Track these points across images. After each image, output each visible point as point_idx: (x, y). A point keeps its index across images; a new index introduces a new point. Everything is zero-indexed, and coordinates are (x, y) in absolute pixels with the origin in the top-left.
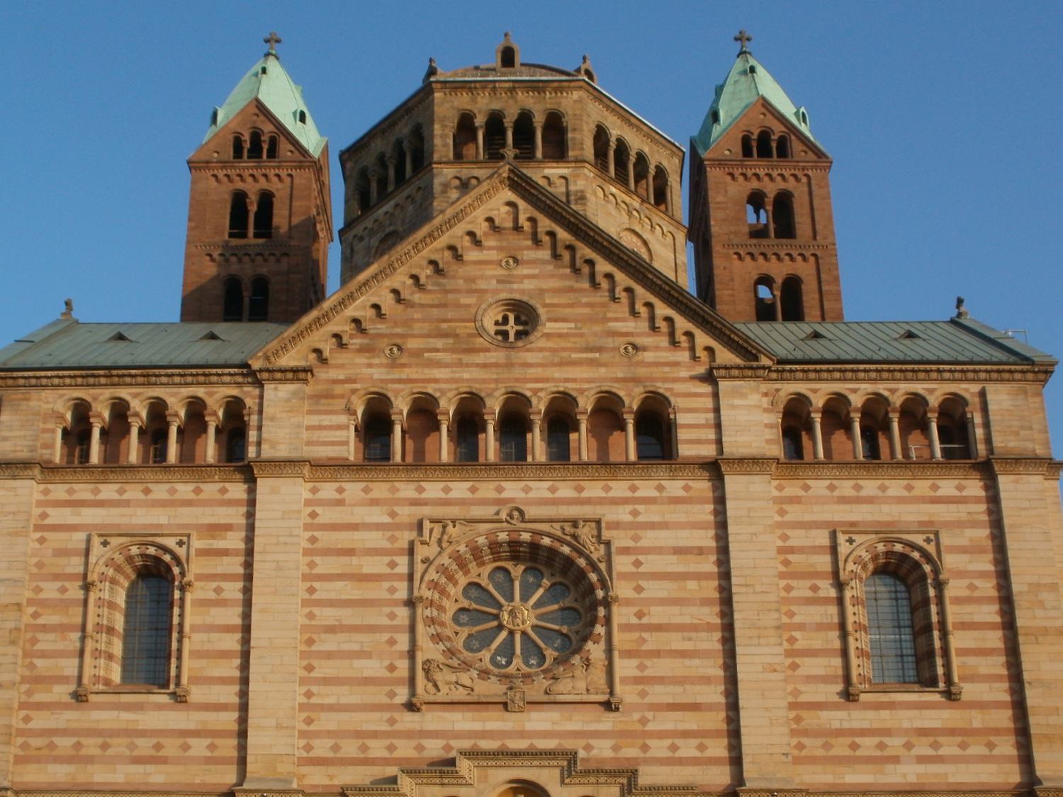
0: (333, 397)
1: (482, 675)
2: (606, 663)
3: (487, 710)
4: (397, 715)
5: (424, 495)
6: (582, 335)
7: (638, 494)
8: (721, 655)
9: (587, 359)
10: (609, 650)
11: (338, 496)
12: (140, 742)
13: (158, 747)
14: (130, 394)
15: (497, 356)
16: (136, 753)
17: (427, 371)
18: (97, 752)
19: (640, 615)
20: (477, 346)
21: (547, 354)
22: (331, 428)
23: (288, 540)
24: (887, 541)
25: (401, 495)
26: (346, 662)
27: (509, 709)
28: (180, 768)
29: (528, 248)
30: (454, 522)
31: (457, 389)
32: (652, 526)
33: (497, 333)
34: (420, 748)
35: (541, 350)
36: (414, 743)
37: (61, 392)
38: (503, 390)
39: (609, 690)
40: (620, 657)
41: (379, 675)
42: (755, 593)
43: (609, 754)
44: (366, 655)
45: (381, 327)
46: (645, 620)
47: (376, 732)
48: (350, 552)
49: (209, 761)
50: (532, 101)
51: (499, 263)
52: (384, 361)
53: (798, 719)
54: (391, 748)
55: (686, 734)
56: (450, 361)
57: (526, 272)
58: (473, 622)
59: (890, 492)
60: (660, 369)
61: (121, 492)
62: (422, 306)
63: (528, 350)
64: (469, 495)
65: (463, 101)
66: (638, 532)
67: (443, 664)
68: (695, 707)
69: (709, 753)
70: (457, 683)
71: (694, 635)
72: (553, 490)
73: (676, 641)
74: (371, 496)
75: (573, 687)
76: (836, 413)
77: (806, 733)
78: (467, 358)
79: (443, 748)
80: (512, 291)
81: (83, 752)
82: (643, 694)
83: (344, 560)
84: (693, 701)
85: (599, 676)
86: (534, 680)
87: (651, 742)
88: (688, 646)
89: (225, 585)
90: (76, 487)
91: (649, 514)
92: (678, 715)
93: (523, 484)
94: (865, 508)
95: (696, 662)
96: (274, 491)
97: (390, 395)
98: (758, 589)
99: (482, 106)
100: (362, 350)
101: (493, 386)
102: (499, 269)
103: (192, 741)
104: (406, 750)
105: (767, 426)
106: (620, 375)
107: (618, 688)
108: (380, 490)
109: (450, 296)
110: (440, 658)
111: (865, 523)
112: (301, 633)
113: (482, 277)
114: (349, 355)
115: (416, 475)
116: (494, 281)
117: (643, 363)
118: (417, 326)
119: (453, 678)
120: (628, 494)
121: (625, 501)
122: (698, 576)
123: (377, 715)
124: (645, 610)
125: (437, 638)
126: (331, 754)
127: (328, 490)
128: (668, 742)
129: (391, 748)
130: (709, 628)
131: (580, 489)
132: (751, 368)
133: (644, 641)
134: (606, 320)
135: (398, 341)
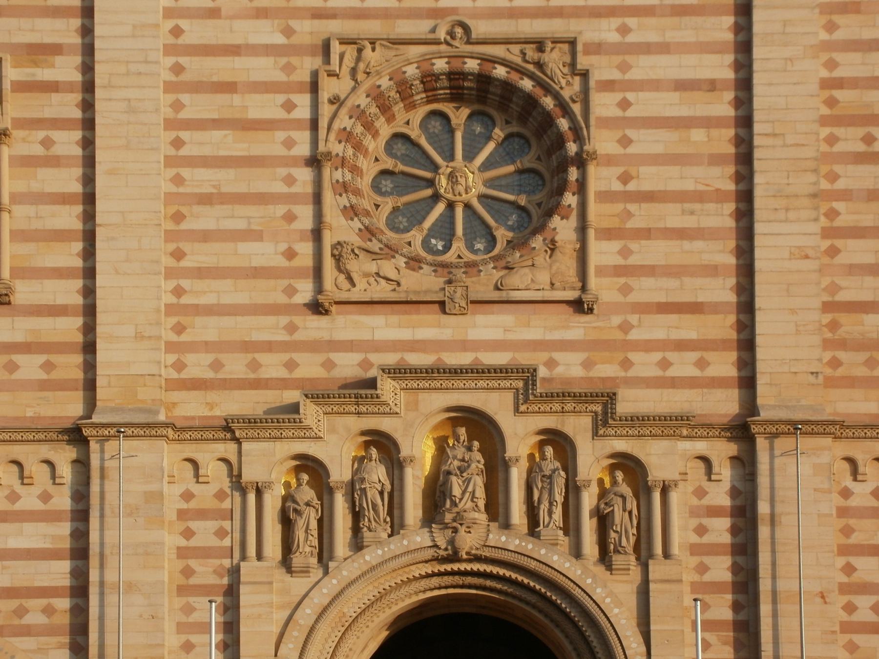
1: (412, 263)
2: (578, 246)
3: (418, 313)
8: (734, 235)
10: (582, 229)
27: (447, 310)
39: (580, 284)
40: (596, 239)
58: (399, 191)
67: (359, 248)
70: (378, 274)
75: (532, 280)
85: (567, 264)
86: (480, 271)
95: (699, 245)
107: (593, 281)
110: (355, 240)
112: (165, 205)
119: (372, 267)
125: (351, 212)
130: (719, 196)
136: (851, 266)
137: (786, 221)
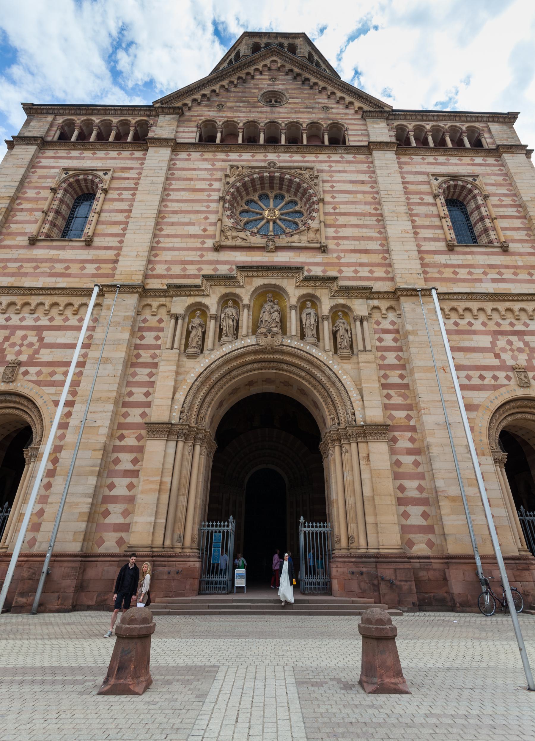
0: (191, 121)
4: (204, 253)
5: (229, 158)
6: (304, 103)
7: (331, 159)
11: (187, 157)
16: (53, 271)
18: (31, 270)
19: (335, 208)
22: (188, 132)
23: (159, 171)
25: (218, 157)
26: (181, 227)
28: (77, 280)
32: (340, 172)
34: (216, 270)
36: (213, 267)
38: (268, 120)
44: (193, 224)
46: (337, 211)
47: (192, 261)
48: (191, 179)
55: (362, 265)
65: (257, 40)
68: (366, 251)
69: (375, 275)
71: (363, 218)
72: (291, 157)
73: (354, 220)
78: (252, 110)
79: (228, 270)
82: (338, 245)
83: (187, 182)
92: (358, 255)
93: (277, 154)
94: (440, 167)
98: (394, 196)
100: (205, 106)
104: (208, 270)
106: (322, 117)
108: (208, 155)
115: (225, 149)
117: (332, 113)
120: (327, 159)
121: (325, 162)
122: (364, 193)
123: (195, 253)
124: (337, 206)
126: (165, 273)
127: (183, 155)
128: (353, 268)
133: (337, 220)
134: (314, 98)
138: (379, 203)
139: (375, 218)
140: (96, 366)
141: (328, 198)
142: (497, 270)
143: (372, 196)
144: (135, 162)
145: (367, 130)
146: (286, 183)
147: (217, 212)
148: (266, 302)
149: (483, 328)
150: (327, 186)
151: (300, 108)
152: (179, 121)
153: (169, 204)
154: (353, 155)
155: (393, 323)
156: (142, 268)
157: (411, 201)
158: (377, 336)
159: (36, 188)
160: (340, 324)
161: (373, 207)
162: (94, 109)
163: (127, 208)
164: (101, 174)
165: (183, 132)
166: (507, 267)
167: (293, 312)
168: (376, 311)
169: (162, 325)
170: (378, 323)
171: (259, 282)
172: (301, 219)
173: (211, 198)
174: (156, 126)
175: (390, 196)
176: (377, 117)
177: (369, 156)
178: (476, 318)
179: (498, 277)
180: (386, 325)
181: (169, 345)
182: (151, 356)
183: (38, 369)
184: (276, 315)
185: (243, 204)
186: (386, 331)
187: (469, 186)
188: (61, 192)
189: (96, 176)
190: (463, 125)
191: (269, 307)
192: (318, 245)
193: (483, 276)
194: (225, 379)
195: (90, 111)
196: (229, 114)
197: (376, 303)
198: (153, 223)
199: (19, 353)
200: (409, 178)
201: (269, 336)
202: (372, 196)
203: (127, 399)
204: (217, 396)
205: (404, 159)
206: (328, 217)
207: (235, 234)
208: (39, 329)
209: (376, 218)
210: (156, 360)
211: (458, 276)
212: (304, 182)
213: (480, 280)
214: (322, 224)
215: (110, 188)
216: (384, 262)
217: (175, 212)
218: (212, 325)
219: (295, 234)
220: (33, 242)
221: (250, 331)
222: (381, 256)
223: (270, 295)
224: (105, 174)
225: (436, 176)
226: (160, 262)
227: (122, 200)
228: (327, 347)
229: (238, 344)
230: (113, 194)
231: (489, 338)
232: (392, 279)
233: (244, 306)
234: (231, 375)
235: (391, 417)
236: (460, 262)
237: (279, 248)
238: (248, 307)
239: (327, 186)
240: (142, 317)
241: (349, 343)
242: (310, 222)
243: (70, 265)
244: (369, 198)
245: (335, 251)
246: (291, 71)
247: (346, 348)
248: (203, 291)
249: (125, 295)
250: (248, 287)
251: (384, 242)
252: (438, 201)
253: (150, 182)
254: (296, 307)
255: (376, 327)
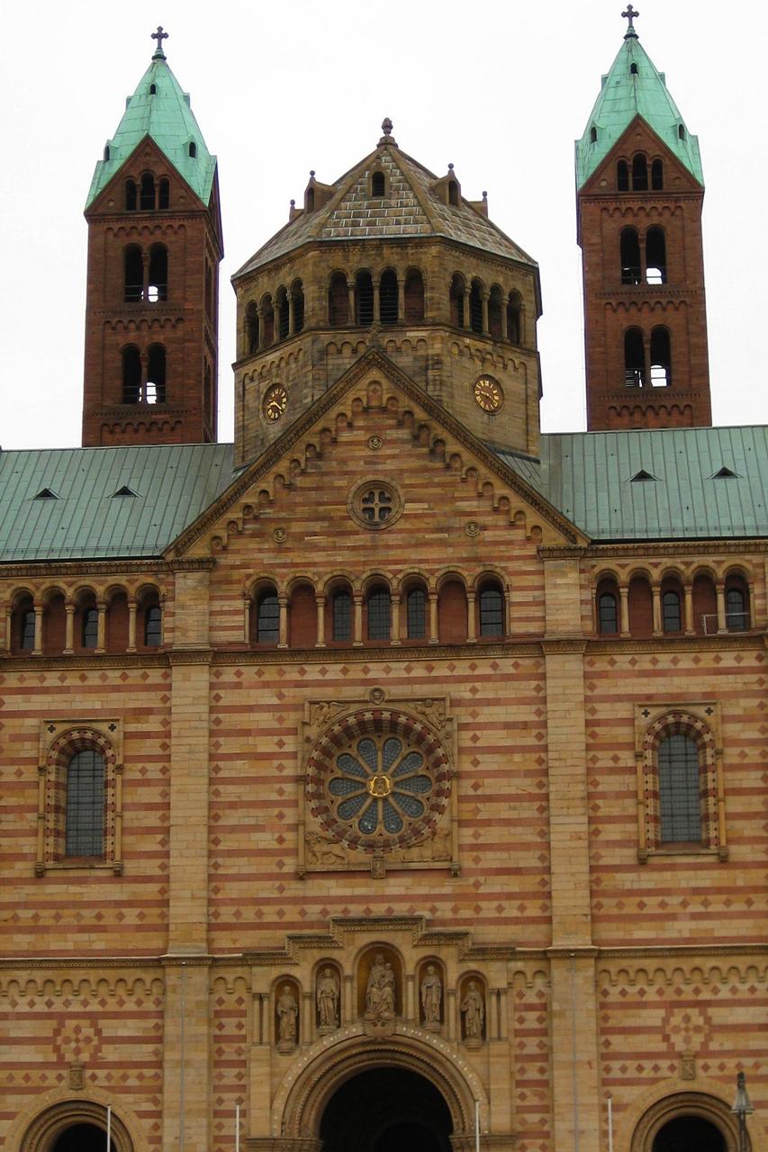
0: (231, 582)
6: (433, 516)
7: (478, 672)
9: (437, 539)
11: (237, 680)
12: (85, 912)
13: (99, 917)
14: (66, 583)
15: (363, 539)
16: (83, 922)
17: (307, 554)
19: (476, 787)
20: (349, 529)
21: (404, 535)
23: (197, 724)
24: (675, 713)
25: (288, 677)
28: (117, 936)
29: (391, 427)
30: (328, 703)
31: (331, 572)
33: (365, 510)
34: (303, 913)
35: (400, 531)
36: (298, 908)
37: (9, 581)
38: (369, 573)
41: (270, 847)
42: (566, 766)
43: (449, 915)
45: (269, 512)
46: (479, 792)
48: (247, 733)
49: (139, 928)
50: (396, 257)
51: (366, 443)
52: (273, 546)
53: (598, 881)
54: (281, 913)
56: (325, 544)
57: (388, 452)
59: (681, 665)
60: (497, 548)
61: (62, 679)
62: (303, 489)
63: (389, 532)
64: (341, 676)
66: (476, 708)
68: (517, 871)
71: (518, 804)
72: (408, 670)
73: (503, 811)
74: (264, 678)
76: (640, 581)
77: (604, 894)
80: (376, 472)
81: (41, 923)
82: (477, 860)
83: (242, 740)
84: (515, 866)
87: (483, 904)
88: (513, 815)
89: (149, 766)
90: (25, 674)
91: (486, 691)
92: (504, 878)
94: (660, 680)
95: (519, 830)
96: (186, 679)
97: (277, 579)
98: (569, 762)
99: (352, 264)
100: (252, 536)
101: (361, 568)
102: (367, 449)
103: (125, 911)
104: (292, 914)
105: (582, 602)
106: (465, 555)
108: (271, 674)
109: (326, 479)
110: (317, 829)
111: (660, 696)
113: (353, 458)
114: (244, 541)
116: (362, 463)
118: (299, 509)
120: (468, 672)
122: (524, 749)
123: (269, 884)
126: (234, 920)
127: (228, 675)
128: (495, 903)
129: (281, 913)
131: (430, 669)
132: (570, 549)
133: (478, 811)
135: (284, 526)
136: (608, 842)
137: (568, 815)
138: (546, 773)
139: (536, 805)
140: (179, 1071)
141: (466, 766)
142: (703, 898)
143: (537, 755)
144: (152, 695)
145: (542, 588)
146: (400, 730)
147: (295, 803)
148: (374, 964)
149: (656, 998)
150: (465, 738)
151: (426, 531)
152: (211, 582)
153: (221, 788)
154: (513, 661)
155: (540, 995)
156: (203, 919)
157: (599, 764)
158: (517, 1015)
159: (13, 761)
160: (471, 1001)
161: (536, 780)
162: (60, 567)
163: (158, 799)
164: (104, 727)
165: (222, 613)
166: (719, 890)
167: (410, 984)
168: (520, 976)
169: (243, 1007)
170: (521, 995)
171: (365, 939)
172: (426, 795)
173: (286, 773)
174: (173, 599)
175: (563, 764)
176: (564, 558)
177: (540, 660)
178: (650, 983)
179: (702, 909)
180: (531, 998)
181: (256, 1039)
182: (236, 1052)
183: (106, 1072)
184: (388, 989)
185: (336, 769)
186: (530, 1007)
187: (699, 725)
188: (53, 768)
189: (98, 734)
190: (719, 563)
191: (379, 974)
192: (445, 865)
193: (679, 910)
194: (329, 1076)
195: (54, 571)
196: (295, 557)
197: (520, 965)
198: (205, 836)
199: (77, 1051)
200: (604, 711)
201: (380, 1024)
202: (537, 755)
203: (218, 1108)
204: (319, 1097)
205: (601, 664)
206: (467, 806)
207: (326, 848)
208: (93, 1017)
209: (538, 804)
210: (243, 1057)
211: (644, 912)
212: (429, 731)
213: (673, 917)
214: (455, 824)
215: (126, 759)
216: (541, 889)
217: (232, 805)
218: (307, 1008)
219: (414, 845)
220: (40, 875)
221: (356, 1011)
222: (538, 878)
223: (380, 957)
224: (112, 728)
225: (645, 702)
226: (224, 902)
227: (146, 783)
228: (452, 1036)
229: (341, 1035)
230: (133, 772)
231: (662, 1012)
232: (549, 920)
233: (346, 978)
234: (336, 1070)
235: (523, 1122)
236: (651, 885)
237: (390, 872)
238: (350, 978)
239: (465, 738)
240: (216, 997)
241: (480, 1028)
242: (437, 817)
243: (103, 911)
244: (530, 762)
245: (473, 872)
246: (410, 413)
247: (474, 1036)
248: (291, 959)
249: (191, 969)
250: (350, 948)
251: (545, 852)
252: (640, 765)
253: (185, 749)
254: (413, 977)
255: (517, 1001)
